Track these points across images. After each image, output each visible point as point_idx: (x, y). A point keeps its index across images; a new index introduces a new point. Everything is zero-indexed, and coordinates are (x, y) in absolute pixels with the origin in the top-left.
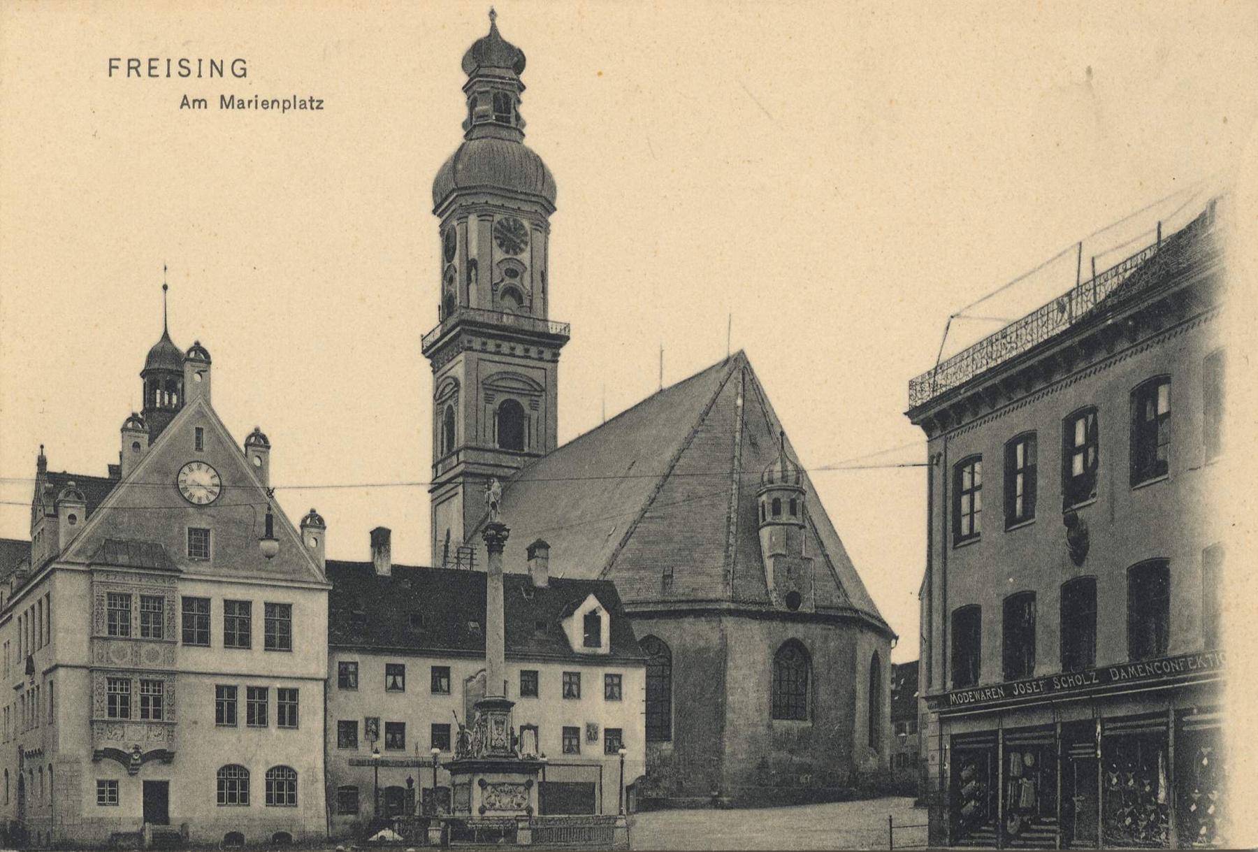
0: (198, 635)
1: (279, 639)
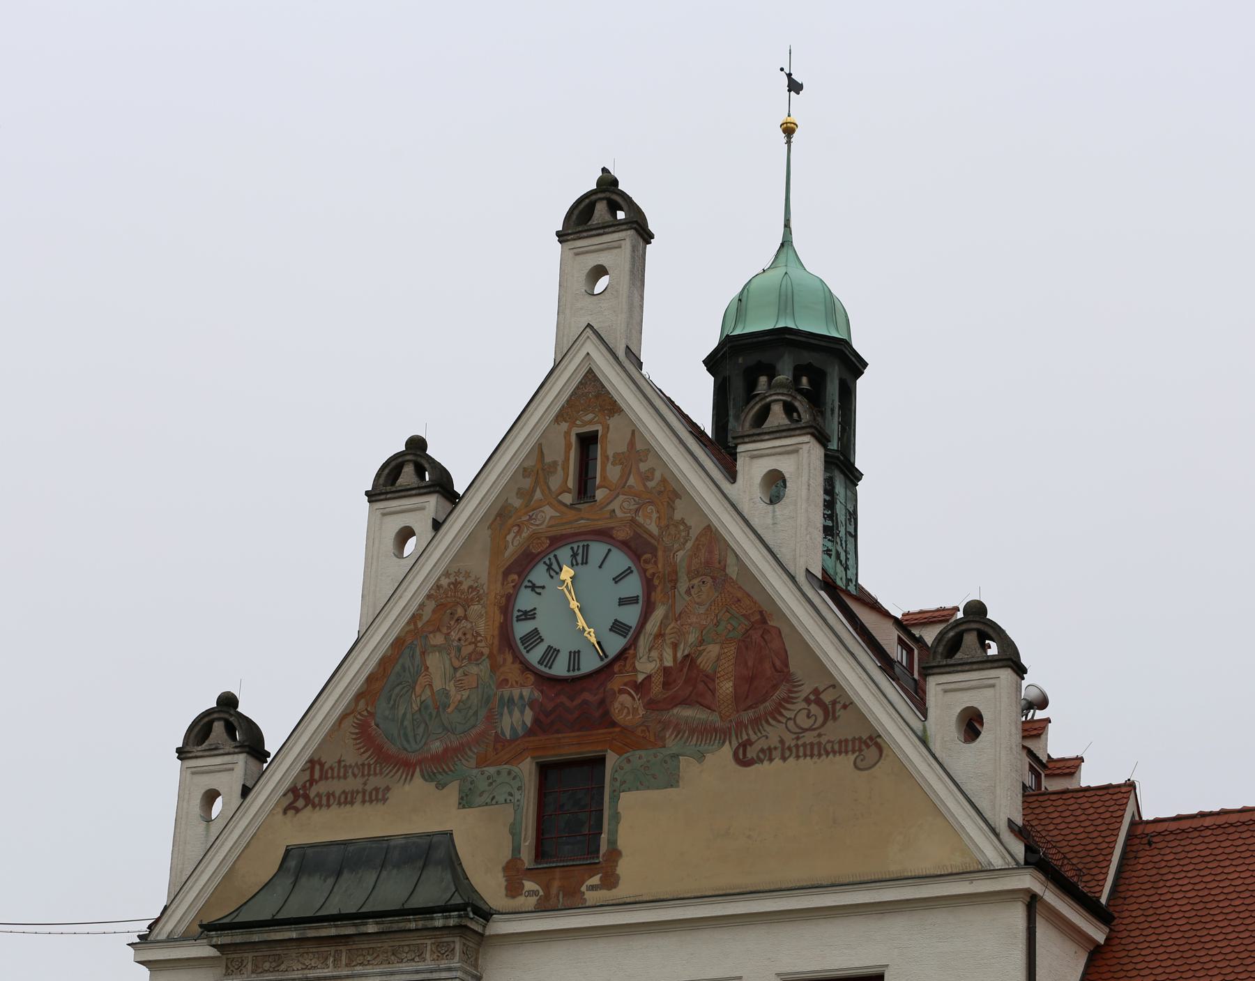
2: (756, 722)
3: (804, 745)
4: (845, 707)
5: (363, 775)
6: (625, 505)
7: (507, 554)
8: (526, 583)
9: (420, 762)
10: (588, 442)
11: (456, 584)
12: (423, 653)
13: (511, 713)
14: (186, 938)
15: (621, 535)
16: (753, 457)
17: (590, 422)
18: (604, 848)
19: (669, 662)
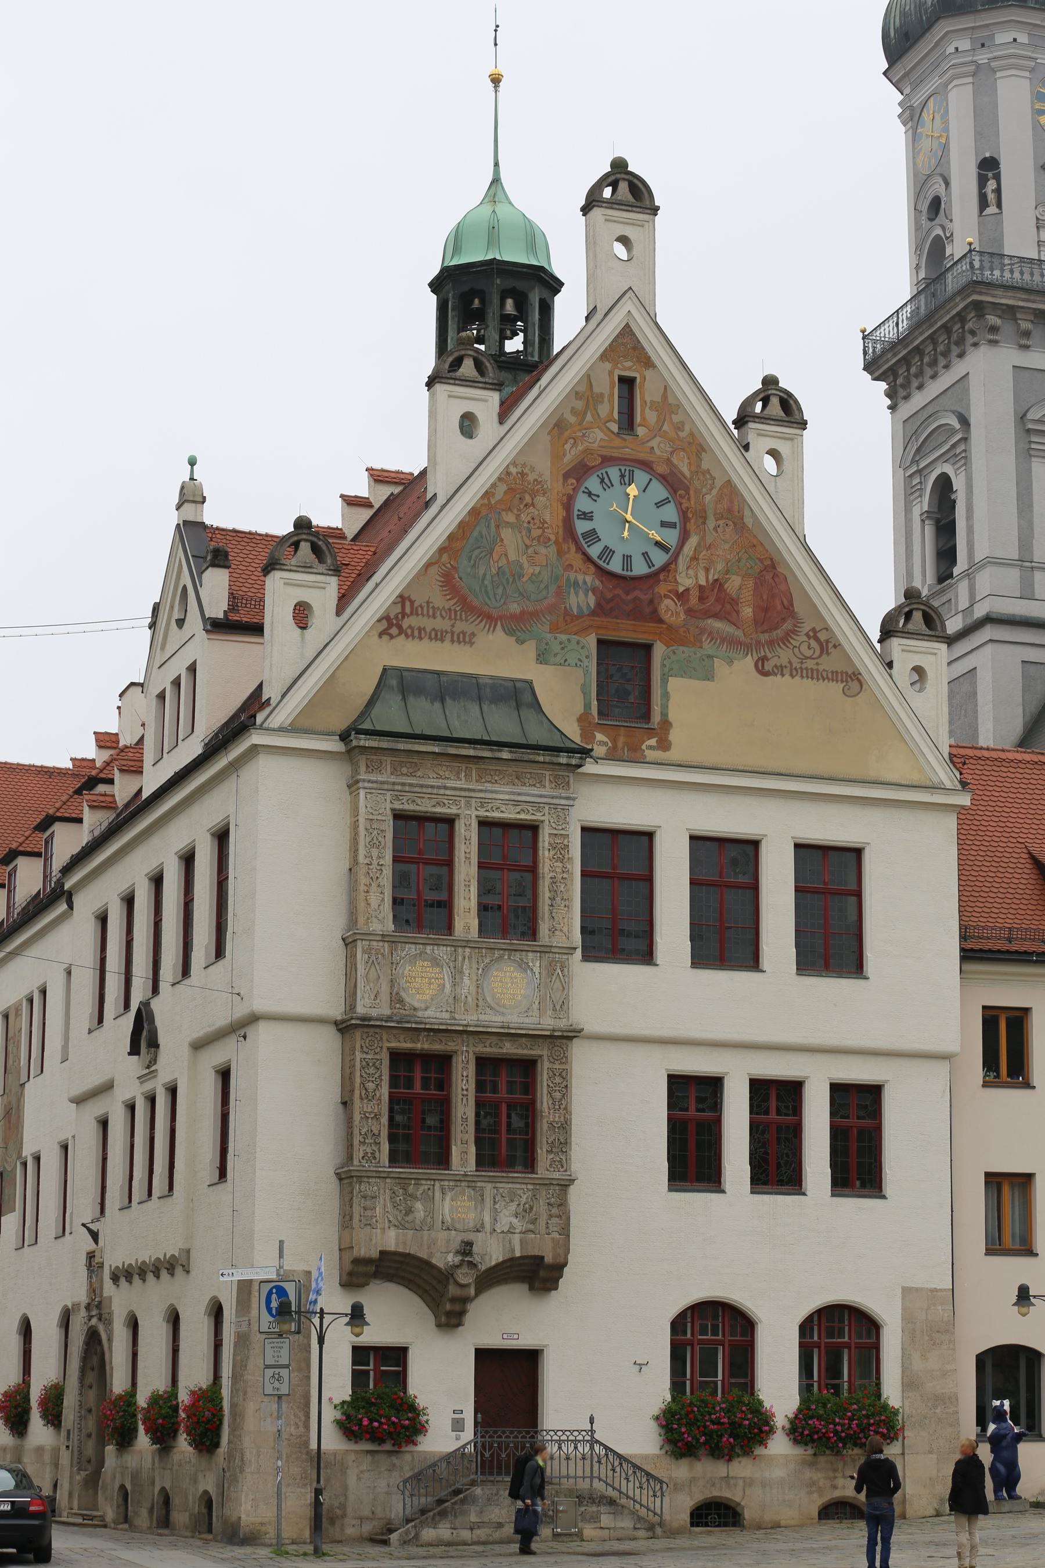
0: (620, 933)
1: (833, 943)
2: (771, 643)
3: (807, 669)
4: (835, 646)
5: (450, 618)
6: (662, 445)
7: (566, 460)
8: (583, 489)
9: (501, 618)
10: (627, 383)
11: (523, 474)
12: (497, 526)
13: (577, 594)
14: (293, 729)
15: (661, 469)
16: (759, 435)
17: (630, 369)
18: (656, 718)
19: (703, 583)
